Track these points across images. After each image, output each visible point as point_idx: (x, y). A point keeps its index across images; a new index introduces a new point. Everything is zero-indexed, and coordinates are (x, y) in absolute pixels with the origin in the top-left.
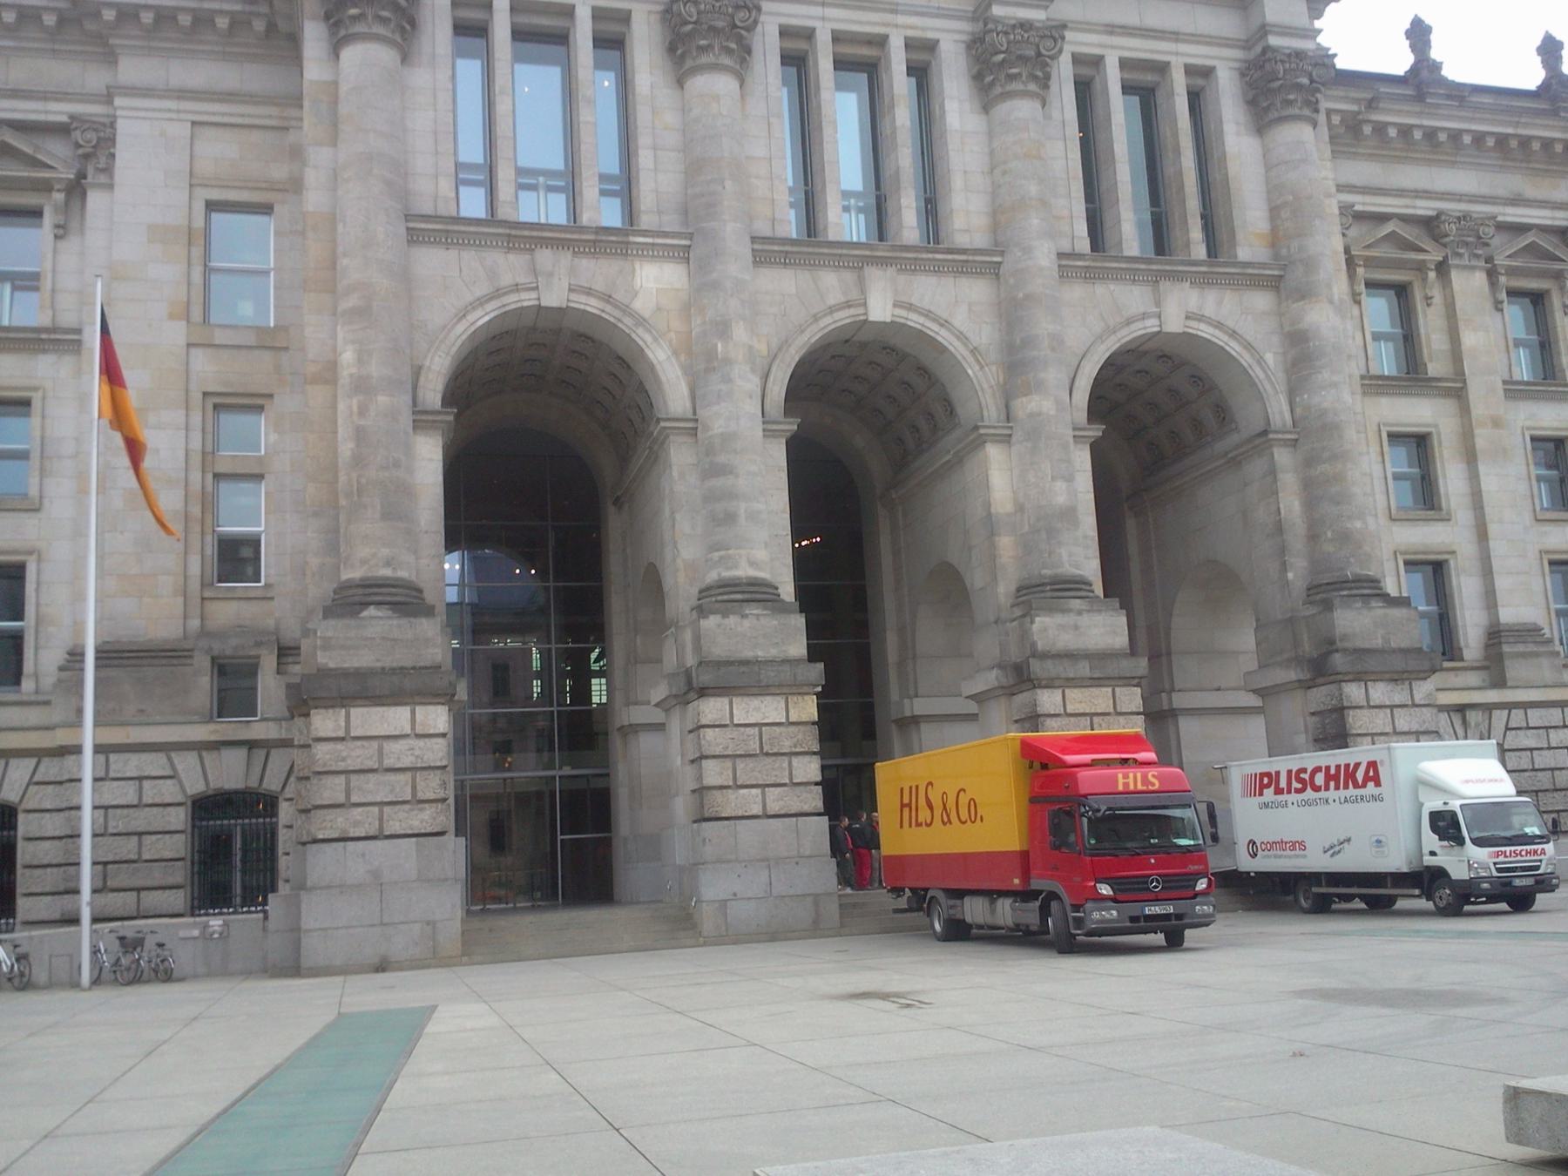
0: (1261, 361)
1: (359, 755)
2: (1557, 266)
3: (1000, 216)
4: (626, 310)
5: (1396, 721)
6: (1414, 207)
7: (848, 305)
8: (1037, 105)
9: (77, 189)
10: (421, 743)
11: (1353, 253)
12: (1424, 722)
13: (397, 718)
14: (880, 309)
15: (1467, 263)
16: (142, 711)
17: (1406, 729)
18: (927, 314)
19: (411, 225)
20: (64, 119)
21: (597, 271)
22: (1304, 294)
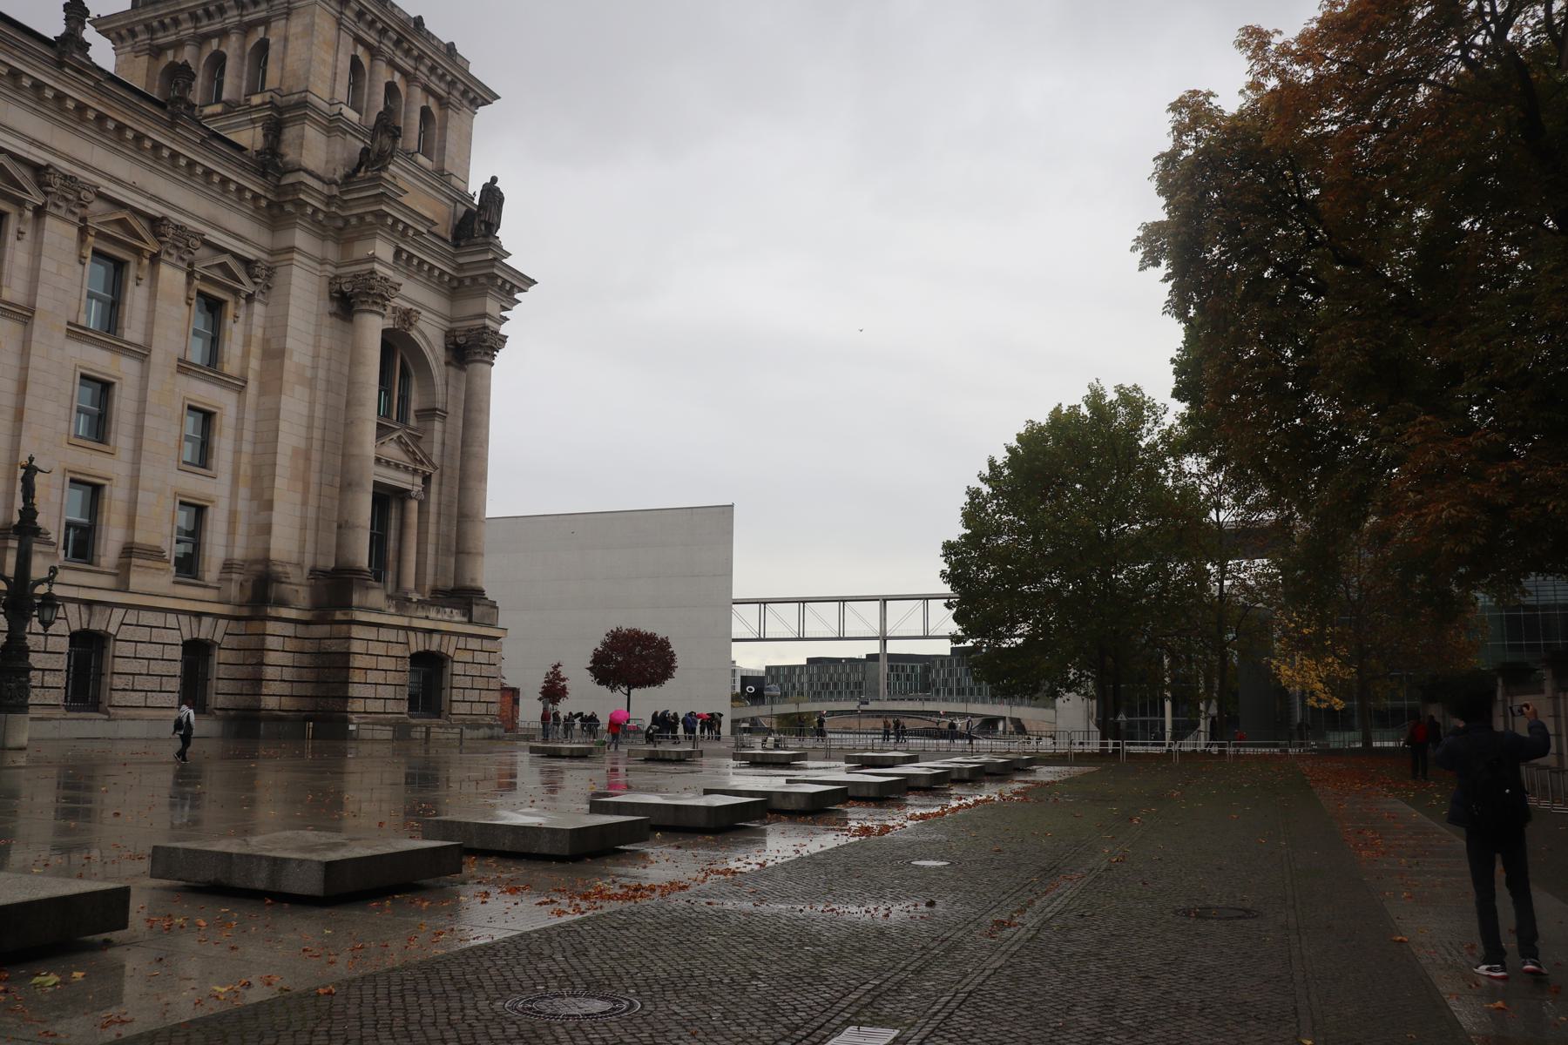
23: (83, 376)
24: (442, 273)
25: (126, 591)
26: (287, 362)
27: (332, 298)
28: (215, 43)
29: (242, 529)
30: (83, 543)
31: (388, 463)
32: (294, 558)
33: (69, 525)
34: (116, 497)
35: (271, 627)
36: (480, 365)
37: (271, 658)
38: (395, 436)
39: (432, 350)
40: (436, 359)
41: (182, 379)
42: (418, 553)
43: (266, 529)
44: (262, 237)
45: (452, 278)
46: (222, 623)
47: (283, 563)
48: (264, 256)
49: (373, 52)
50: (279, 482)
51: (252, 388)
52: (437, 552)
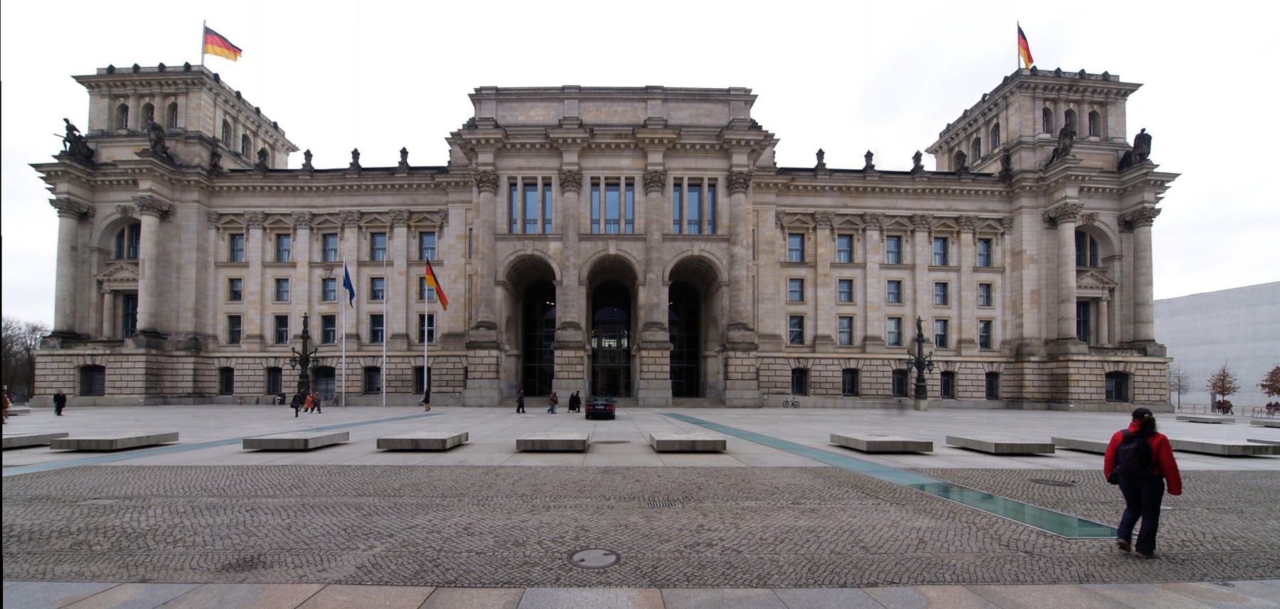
1: (478, 361)
2: (856, 227)
3: (648, 224)
4: (546, 254)
7: (604, 250)
8: (660, 195)
13: (485, 353)
14: (612, 251)
18: (626, 252)
21: (539, 245)
23: (936, 283)
24: (1111, 190)
25: (961, 356)
26: (1024, 256)
27: (1045, 222)
28: (975, 135)
29: (1009, 327)
30: (942, 341)
31: (1086, 287)
32: (1036, 336)
33: (937, 335)
34: (953, 323)
35: (1026, 365)
36: (1142, 228)
37: (1027, 377)
38: (1089, 274)
39: (1110, 228)
40: (1113, 232)
41: (976, 275)
42: (1109, 326)
43: (1021, 326)
44: (1007, 207)
45: (1118, 190)
46: (1003, 366)
47: (1030, 339)
48: (1007, 215)
49: (1055, 101)
50: (1024, 306)
51: (1008, 270)
52: (1121, 324)
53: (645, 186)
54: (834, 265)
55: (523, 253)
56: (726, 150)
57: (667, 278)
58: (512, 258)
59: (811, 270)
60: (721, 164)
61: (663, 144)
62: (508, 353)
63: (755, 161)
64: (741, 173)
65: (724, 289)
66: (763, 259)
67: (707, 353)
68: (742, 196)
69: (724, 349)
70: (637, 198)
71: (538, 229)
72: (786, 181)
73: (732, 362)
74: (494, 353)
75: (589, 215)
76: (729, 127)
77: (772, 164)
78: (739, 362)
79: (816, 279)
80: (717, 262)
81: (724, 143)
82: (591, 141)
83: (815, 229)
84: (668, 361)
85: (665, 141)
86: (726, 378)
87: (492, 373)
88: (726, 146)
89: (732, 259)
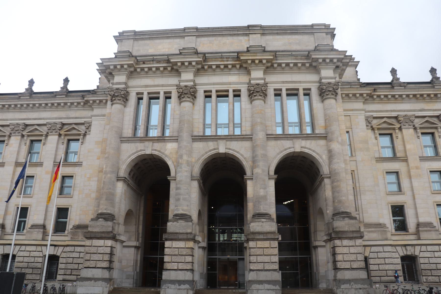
0: (321, 157)
3: (253, 127)
4: (163, 153)
5: (350, 250)
6: (391, 114)
7: (214, 149)
9: (85, 135)
10: (106, 248)
11: (374, 127)
12: (359, 250)
13: (101, 242)
14: (222, 150)
15: (407, 127)
16: (82, 238)
17: (353, 252)
18: (234, 150)
19: (121, 139)
20: (83, 122)
21: (157, 146)
22: (331, 141)
53: (249, 96)
54: (423, 159)
55: (143, 153)
56: (315, 67)
57: (272, 172)
58: (133, 157)
59: (404, 164)
60: (314, 77)
61: (264, 64)
62: (124, 244)
63: (341, 76)
64: (329, 83)
65: (327, 181)
66: (359, 156)
67: (317, 243)
68: (333, 101)
69: (331, 239)
70: (243, 106)
71: (154, 133)
72: (370, 92)
73: (338, 250)
74: (109, 243)
75: (201, 120)
76: (316, 49)
77: (356, 80)
78: (345, 250)
79: (409, 172)
80: (317, 157)
81: (312, 61)
82: (204, 64)
83: (400, 129)
84: (276, 251)
85: (264, 61)
86: (336, 269)
87: (106, 263)
88: (314, 64)
89: (331, 154)
